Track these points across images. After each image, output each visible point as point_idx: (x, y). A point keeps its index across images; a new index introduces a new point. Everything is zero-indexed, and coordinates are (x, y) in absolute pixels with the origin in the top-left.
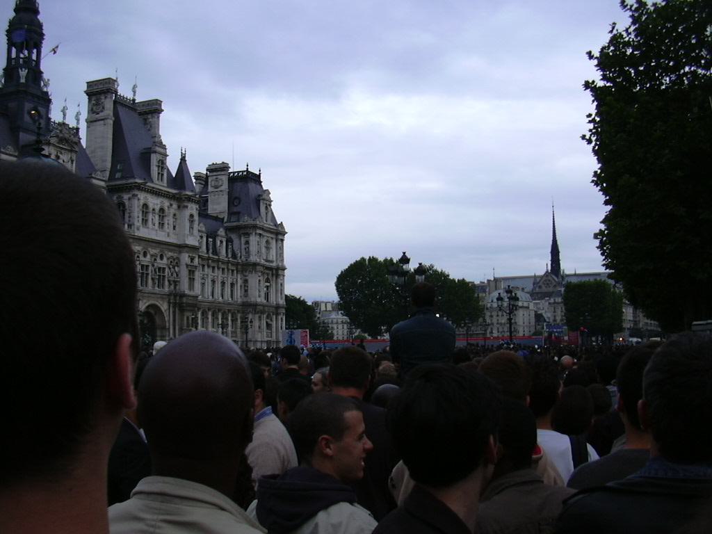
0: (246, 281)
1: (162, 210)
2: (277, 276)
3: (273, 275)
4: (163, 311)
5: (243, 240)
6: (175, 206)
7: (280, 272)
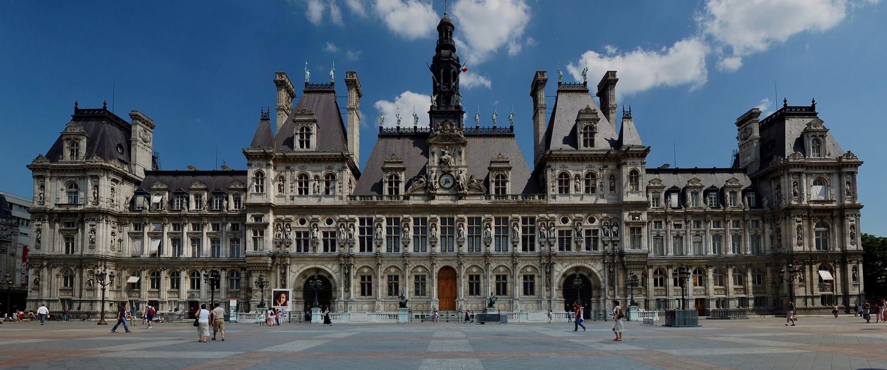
0: (779, 230)
3: (832, 218)
4: (596, 271)
5: (774, 185)
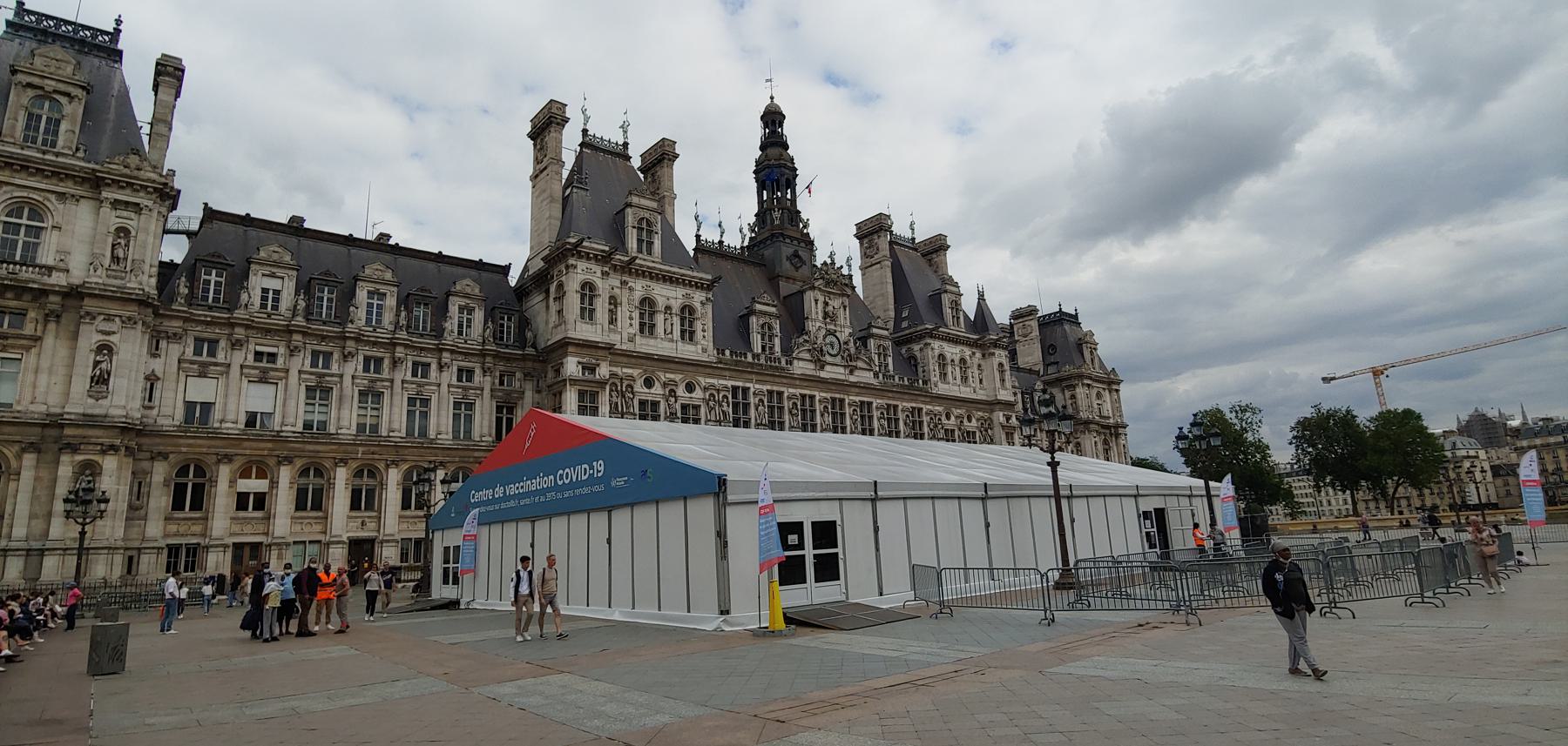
1: (963, 360)
2: (1117, 435)
5: (1068, 394)
6: (978, 355)
7: (1121, 430)
